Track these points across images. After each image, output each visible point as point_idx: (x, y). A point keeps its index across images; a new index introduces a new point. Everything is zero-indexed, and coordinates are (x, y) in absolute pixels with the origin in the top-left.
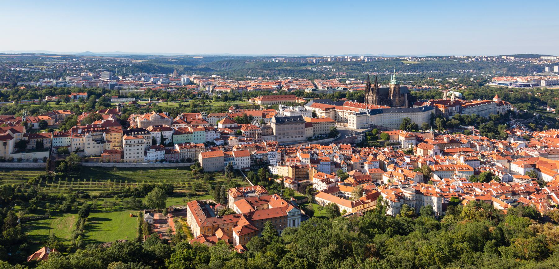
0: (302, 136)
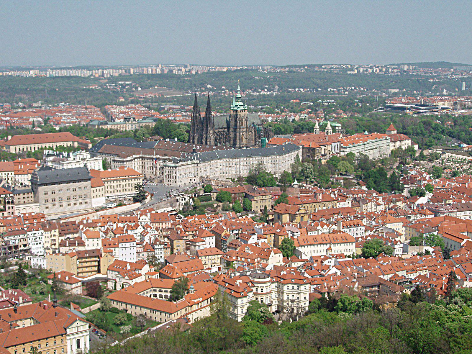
0: (86, 203)
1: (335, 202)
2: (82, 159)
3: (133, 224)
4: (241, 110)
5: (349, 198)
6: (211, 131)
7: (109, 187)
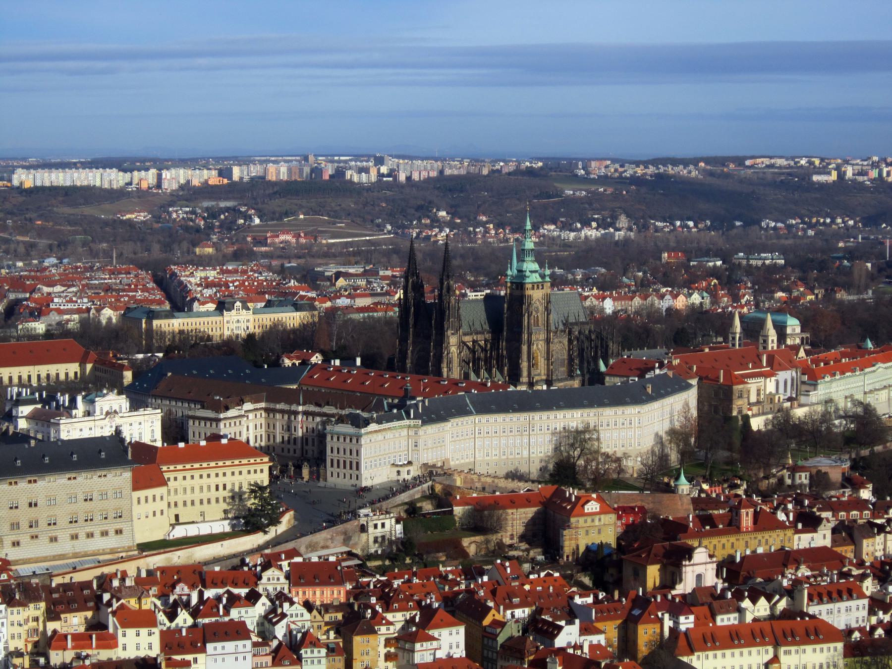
0: (119, 532)
1: (789, 533)
2: (108, 413)
3: (243, 592)
4: (533, 283)
5: (824, 522)
6: (453, 340)
7: (180, 490)
